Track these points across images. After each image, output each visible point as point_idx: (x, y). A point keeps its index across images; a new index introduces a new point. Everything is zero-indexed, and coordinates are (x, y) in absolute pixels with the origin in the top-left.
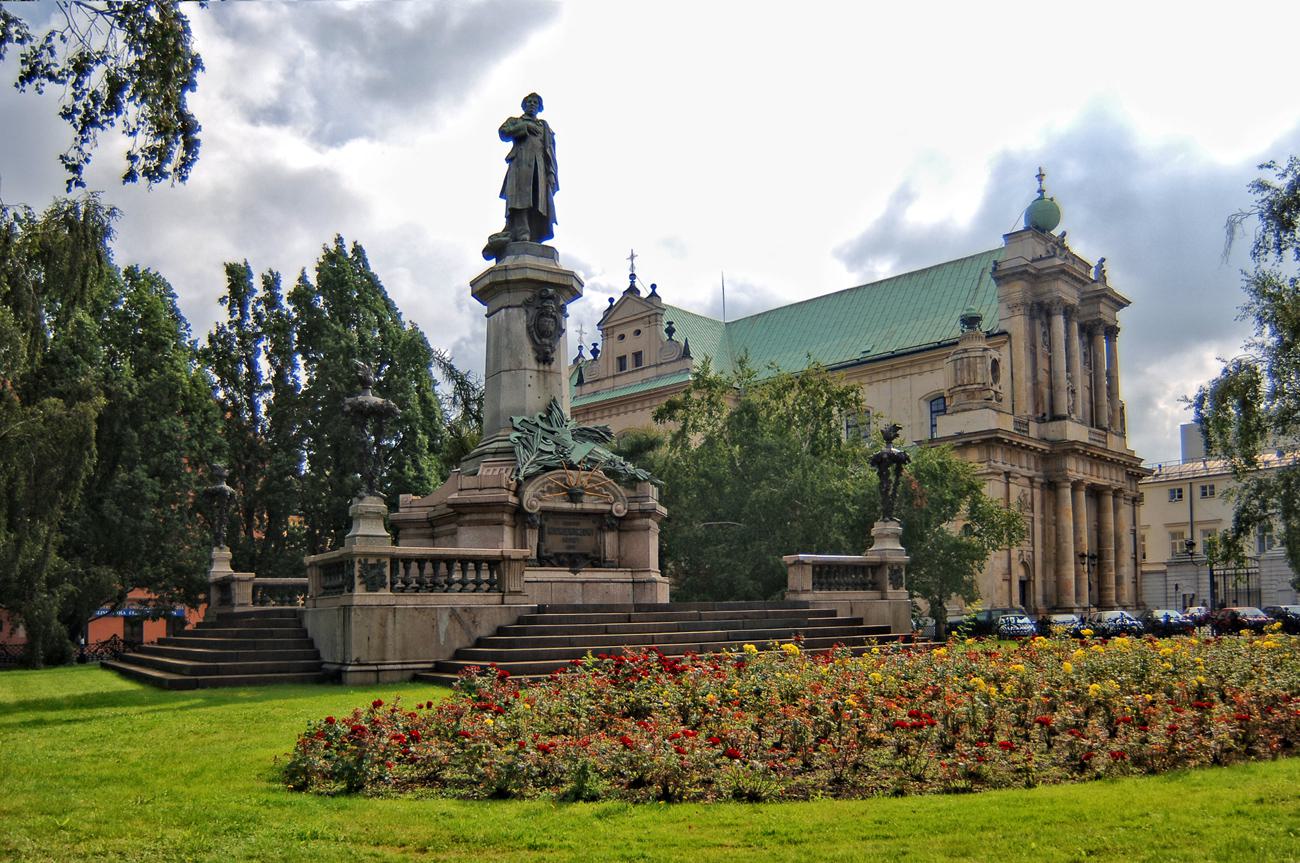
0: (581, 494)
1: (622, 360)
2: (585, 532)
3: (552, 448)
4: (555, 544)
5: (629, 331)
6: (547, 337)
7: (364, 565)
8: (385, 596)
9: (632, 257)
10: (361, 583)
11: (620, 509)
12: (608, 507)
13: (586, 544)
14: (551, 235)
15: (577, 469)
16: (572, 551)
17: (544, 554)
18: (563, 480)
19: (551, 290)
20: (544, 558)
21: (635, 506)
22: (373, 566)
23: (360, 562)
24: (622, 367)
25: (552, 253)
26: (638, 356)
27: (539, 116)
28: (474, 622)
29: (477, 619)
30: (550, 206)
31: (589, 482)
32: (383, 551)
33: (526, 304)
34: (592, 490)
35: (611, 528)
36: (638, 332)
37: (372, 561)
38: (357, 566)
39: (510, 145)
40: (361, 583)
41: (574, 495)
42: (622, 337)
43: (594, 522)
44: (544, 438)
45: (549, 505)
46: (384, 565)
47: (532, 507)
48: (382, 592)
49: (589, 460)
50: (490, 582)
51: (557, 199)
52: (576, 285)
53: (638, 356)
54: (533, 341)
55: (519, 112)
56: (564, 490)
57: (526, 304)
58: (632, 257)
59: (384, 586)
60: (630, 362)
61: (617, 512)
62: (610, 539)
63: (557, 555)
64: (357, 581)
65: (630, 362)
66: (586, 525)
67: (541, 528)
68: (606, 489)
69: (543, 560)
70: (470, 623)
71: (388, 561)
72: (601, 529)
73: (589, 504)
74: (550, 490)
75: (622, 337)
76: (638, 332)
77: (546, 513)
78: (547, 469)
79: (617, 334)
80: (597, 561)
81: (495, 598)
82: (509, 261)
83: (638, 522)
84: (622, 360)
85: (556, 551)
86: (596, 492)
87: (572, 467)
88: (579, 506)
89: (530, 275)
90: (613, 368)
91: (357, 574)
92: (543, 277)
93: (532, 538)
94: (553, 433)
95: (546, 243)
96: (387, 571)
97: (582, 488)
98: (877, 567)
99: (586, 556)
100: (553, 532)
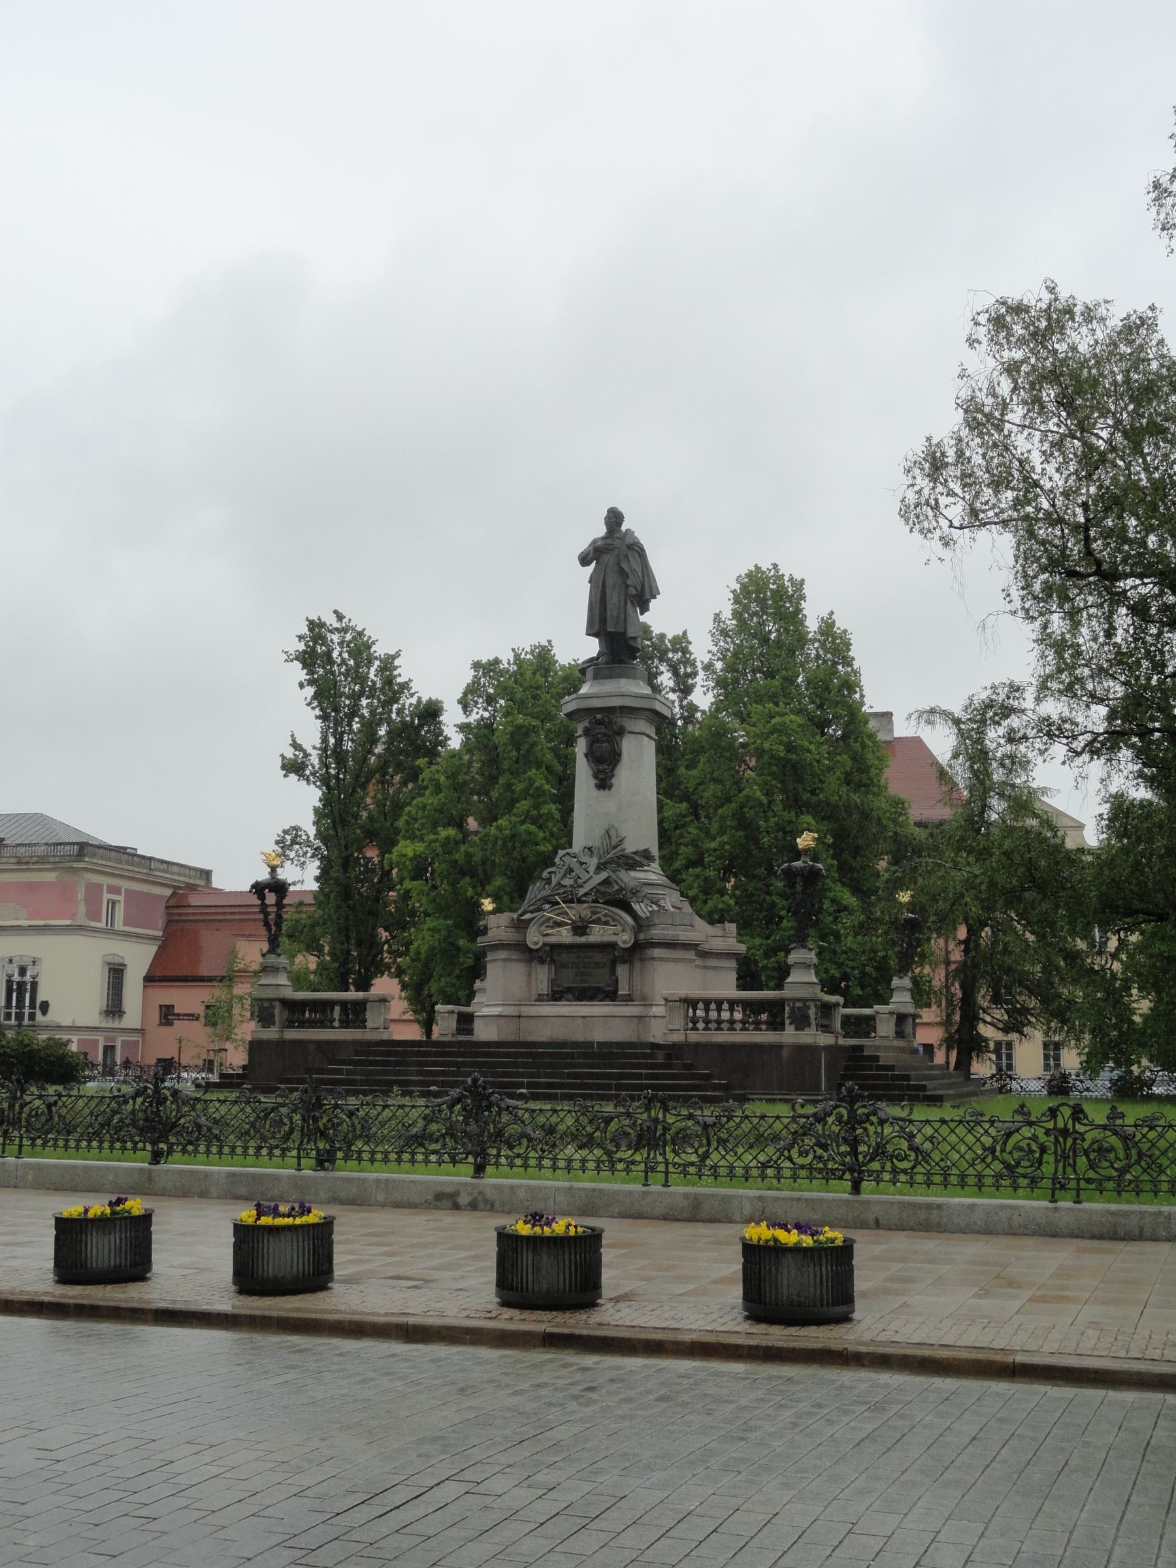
2: (598, 965)
4: (569, 979)
11: (625, 939)
12: (613, 939)
13: (599, 978)
16: (583, 985)
19: (599, 716)
21: (642, 936)
31: (593, 913)
34: (597, 921)
35: (625, 962)
44: (571, 870)
45: (552, 940)
46: (274, 1007)
47: (536, 943)
48: (273, 1029)
49: (598, 891)
61: (624, 942)
62: (622, 971)
63: (569, 990)
66: (598, 957)
67: (553, 961)
68: (614, 920)
69: (556, 996)
73: (598, 934)
80: (611, 995)
85: (566, 985)
88: (583, 939)
94: (582, 863)
99: (598, 990)
100: (564, 966)
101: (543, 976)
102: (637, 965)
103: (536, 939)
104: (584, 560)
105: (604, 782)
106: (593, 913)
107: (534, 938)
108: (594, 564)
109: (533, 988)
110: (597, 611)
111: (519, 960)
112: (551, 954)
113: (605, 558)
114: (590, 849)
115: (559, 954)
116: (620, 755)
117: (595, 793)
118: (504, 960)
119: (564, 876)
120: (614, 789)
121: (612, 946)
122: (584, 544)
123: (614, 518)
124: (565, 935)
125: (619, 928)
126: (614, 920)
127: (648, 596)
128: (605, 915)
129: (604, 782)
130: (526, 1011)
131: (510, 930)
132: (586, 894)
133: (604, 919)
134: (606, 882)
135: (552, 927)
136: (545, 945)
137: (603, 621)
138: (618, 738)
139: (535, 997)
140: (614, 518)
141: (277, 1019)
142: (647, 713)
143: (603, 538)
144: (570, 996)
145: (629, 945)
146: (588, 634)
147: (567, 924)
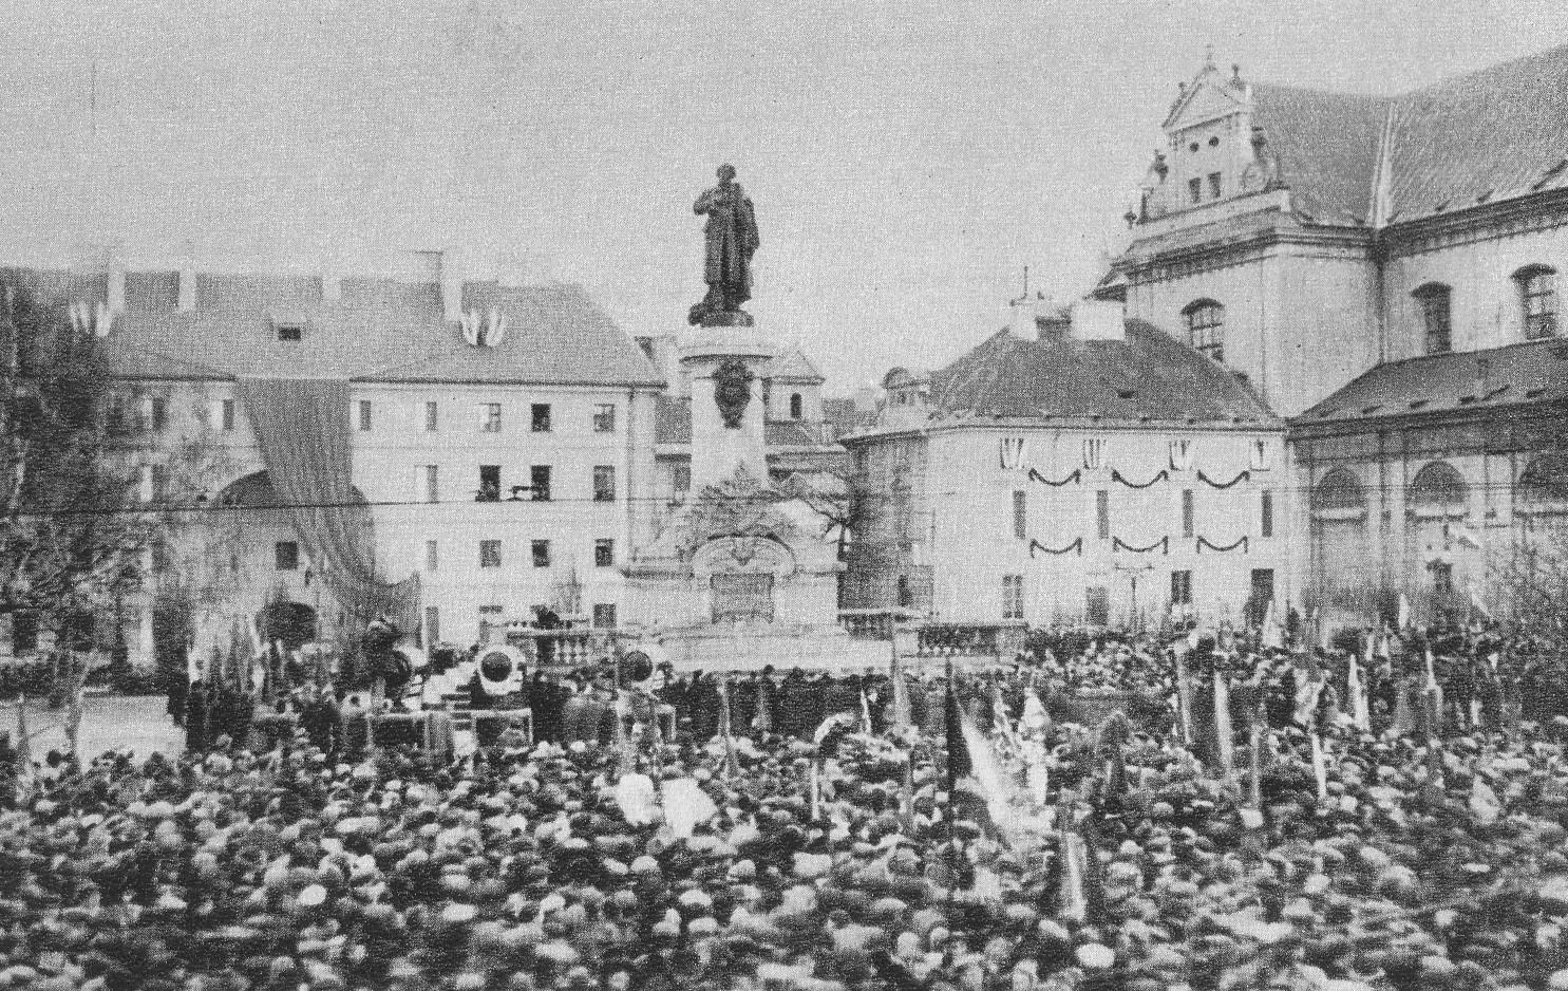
1: (1194, 184)
24: (1197, 199)
26: (1214, 178)
27: (733, 181)
30: (743, 270)
36: (1214, 142)
39: (706, 217)
42: (1195, 147)
51: (755, 265)
53: (1214, 178)
55: (714, 182)
57: (715, 376)
75: (1195, 147)
76: (1214, 142)
79: (1188, 144)
84: (1194, 184)
105: (733, 422)
123: (727, 173)
129: (733, 422)
140: (727, 173)
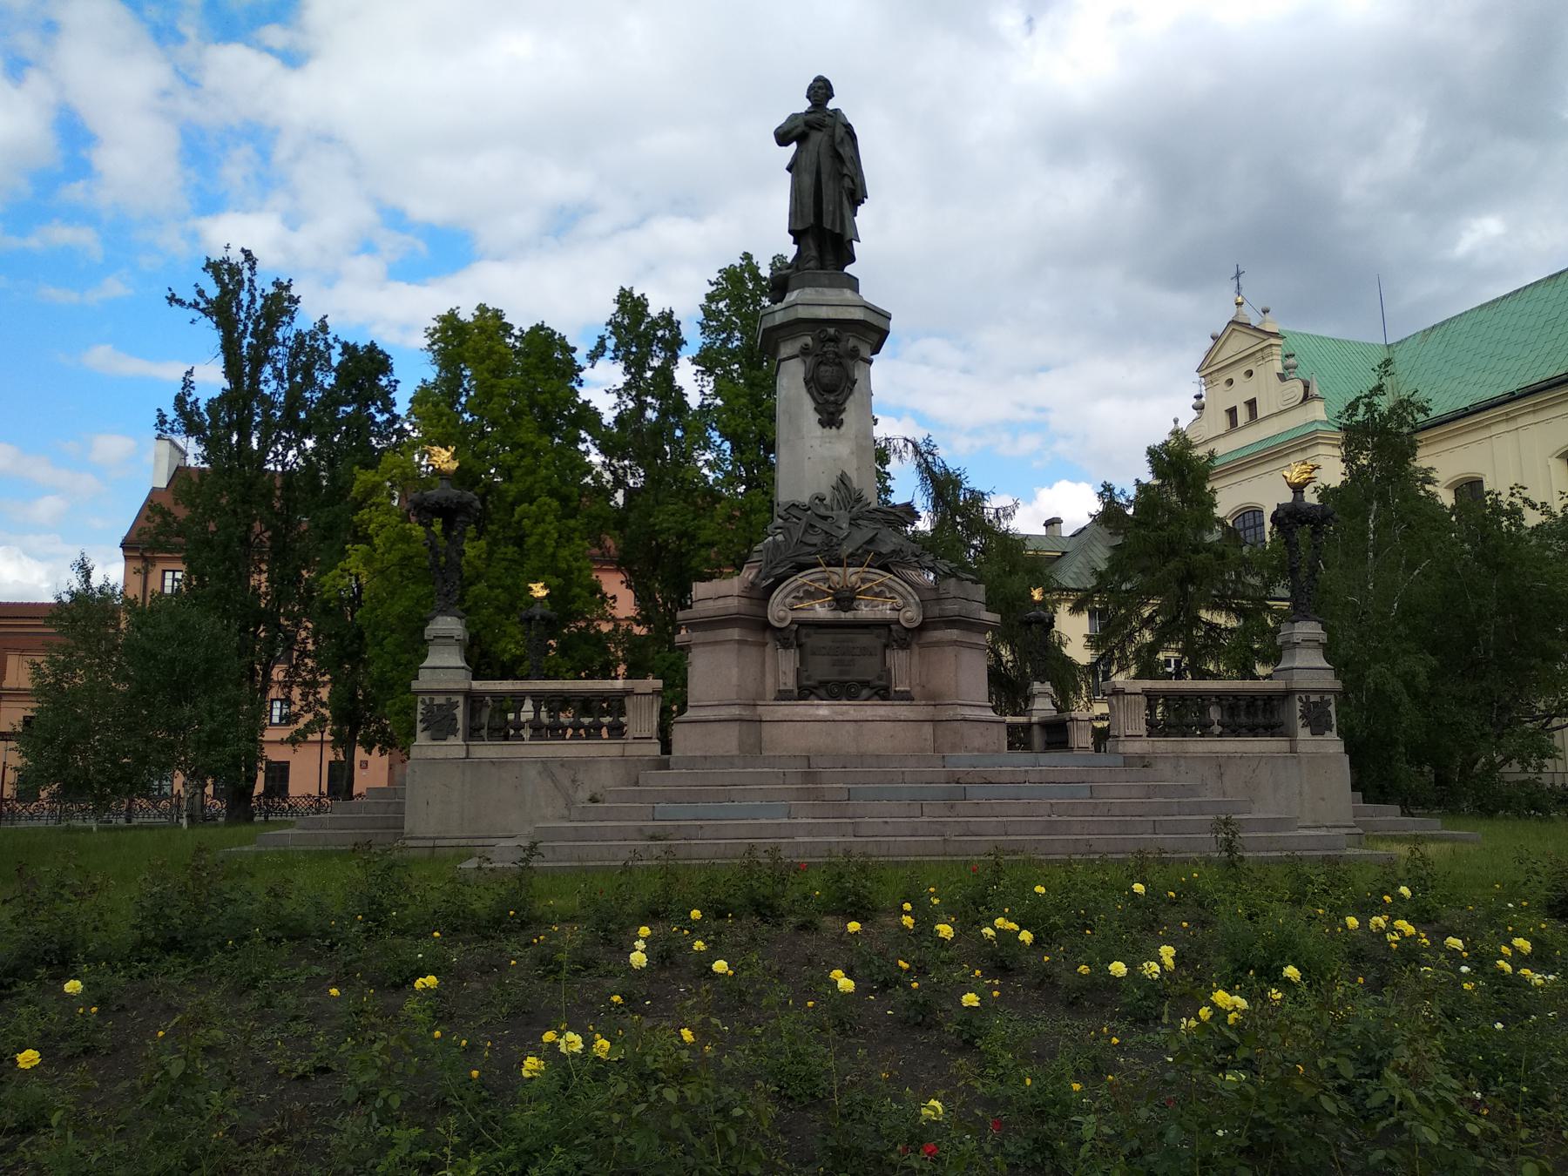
0: (854, 599)
2: (866, 651)
3: (816, 540)
5: (1237, 374)
6: (830, 392)
7: (429, 708)
8: (454, 746)
9: (1238, 276)
10: (424, 730)
11: (911, 615)
12: (894, 615)
13: (866, 668)
14: (852, 259)
15: (849, 565)
17: (806, 683)
18: (826, 580)
19: (832, 331)
20: (807, 688)
21: (935, 611)
22: (439, 706)
23: (423, 702)
25: (853, 283)
26: (1252, 404)
27: (831, 105)
28: (574, 781)
29: (580, 777)
32: (452, 686)
33: (805, 352)
35: (904, 645)
36: (1250, 373)
37: (440, 700)
38: (420, 707)
40: (424, 730)
41: (844, 599)
42: (1230, 382)
43: (878, 637)
44: (812, 526)
45: (803, 615)
47: (782, 620)
48: (452, 740)
50: (611, 728)
52: (872, 318)
54: (814, 399)
55: (804, 105)
56: (829, 595)
57: (805, 352)
58: (1238, 276)
59: (454, 732)
60: (1243, 416)
61: (907, 620)
62: (898, 660)
63: (823, 684)
64: (420, 726)
65: (1243, 416)
66: (864, 639)
67: (800, 646)
69: (805, 691)
70: (567, 783)
71: (460, 699)
72: (886, 646)
73: (865, 611)
74: (811, 595)
77: (803, 624)
78: (801, 567)
80: (884, 693)
81: (612, 749)
82: (791, 297)
83: (938, 635)
84: (1232, 412)
86: (877, 595)
87: (839, 564)
88: (849, 616)
89: (803, 313)
90: (1223, 423)
91: (419, 717)
92: (824, 313)
93: (787, 663)
94: (825, 518)
95: (849, 269)
96: (459, 713)
97: (853, 589)
98: (1288, 694)
99: (865, 684)
101: (787, 663)
102: (916, 648)
103: (782, 614)
104: (783, 138)
105: (831, 418)
106: (864, 581)
107: (779, 610)
108: (794, 146)
109: (769, 681)
110: (809, 201)
111: (754, 644)
112: (797, 635)
113: (817, 137)
114: (822, 500)
115: (808, 636)
116: (855, 382)
117: (818, 430)
118: (738, 642)
119: (806, 531)
120: (843, 429)
121: (885, 625)
122: (780, 120)
123: (821, 90)
124: (821, 611)
125: (899, 601)
126: (891, 589)
127: (859, 196)
128: (881, 584)
130: (765, 712)
131: (744, 601)
132: (851, 555)
133: (877, 589)
134: (871, 541)
135: (801, 599)
136: (792, 622)
137: (819, 214)
138: (851, 363)
139: (770, 693)
140: (821, 90)
141: (460, 725)
142: (876, 337)
143: (807, 113)
144: (822, 692)
145: (916, 624)
146: (791, 232)
147: (824, 594)
